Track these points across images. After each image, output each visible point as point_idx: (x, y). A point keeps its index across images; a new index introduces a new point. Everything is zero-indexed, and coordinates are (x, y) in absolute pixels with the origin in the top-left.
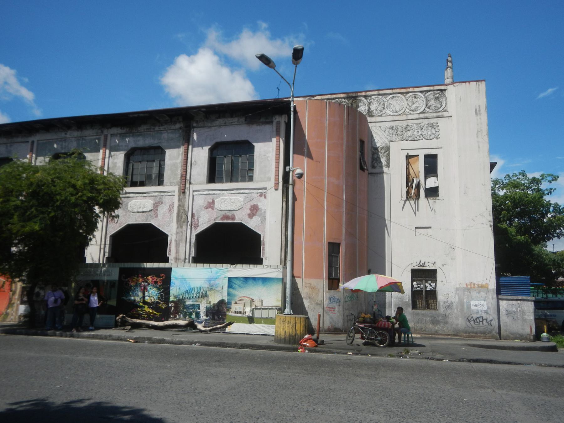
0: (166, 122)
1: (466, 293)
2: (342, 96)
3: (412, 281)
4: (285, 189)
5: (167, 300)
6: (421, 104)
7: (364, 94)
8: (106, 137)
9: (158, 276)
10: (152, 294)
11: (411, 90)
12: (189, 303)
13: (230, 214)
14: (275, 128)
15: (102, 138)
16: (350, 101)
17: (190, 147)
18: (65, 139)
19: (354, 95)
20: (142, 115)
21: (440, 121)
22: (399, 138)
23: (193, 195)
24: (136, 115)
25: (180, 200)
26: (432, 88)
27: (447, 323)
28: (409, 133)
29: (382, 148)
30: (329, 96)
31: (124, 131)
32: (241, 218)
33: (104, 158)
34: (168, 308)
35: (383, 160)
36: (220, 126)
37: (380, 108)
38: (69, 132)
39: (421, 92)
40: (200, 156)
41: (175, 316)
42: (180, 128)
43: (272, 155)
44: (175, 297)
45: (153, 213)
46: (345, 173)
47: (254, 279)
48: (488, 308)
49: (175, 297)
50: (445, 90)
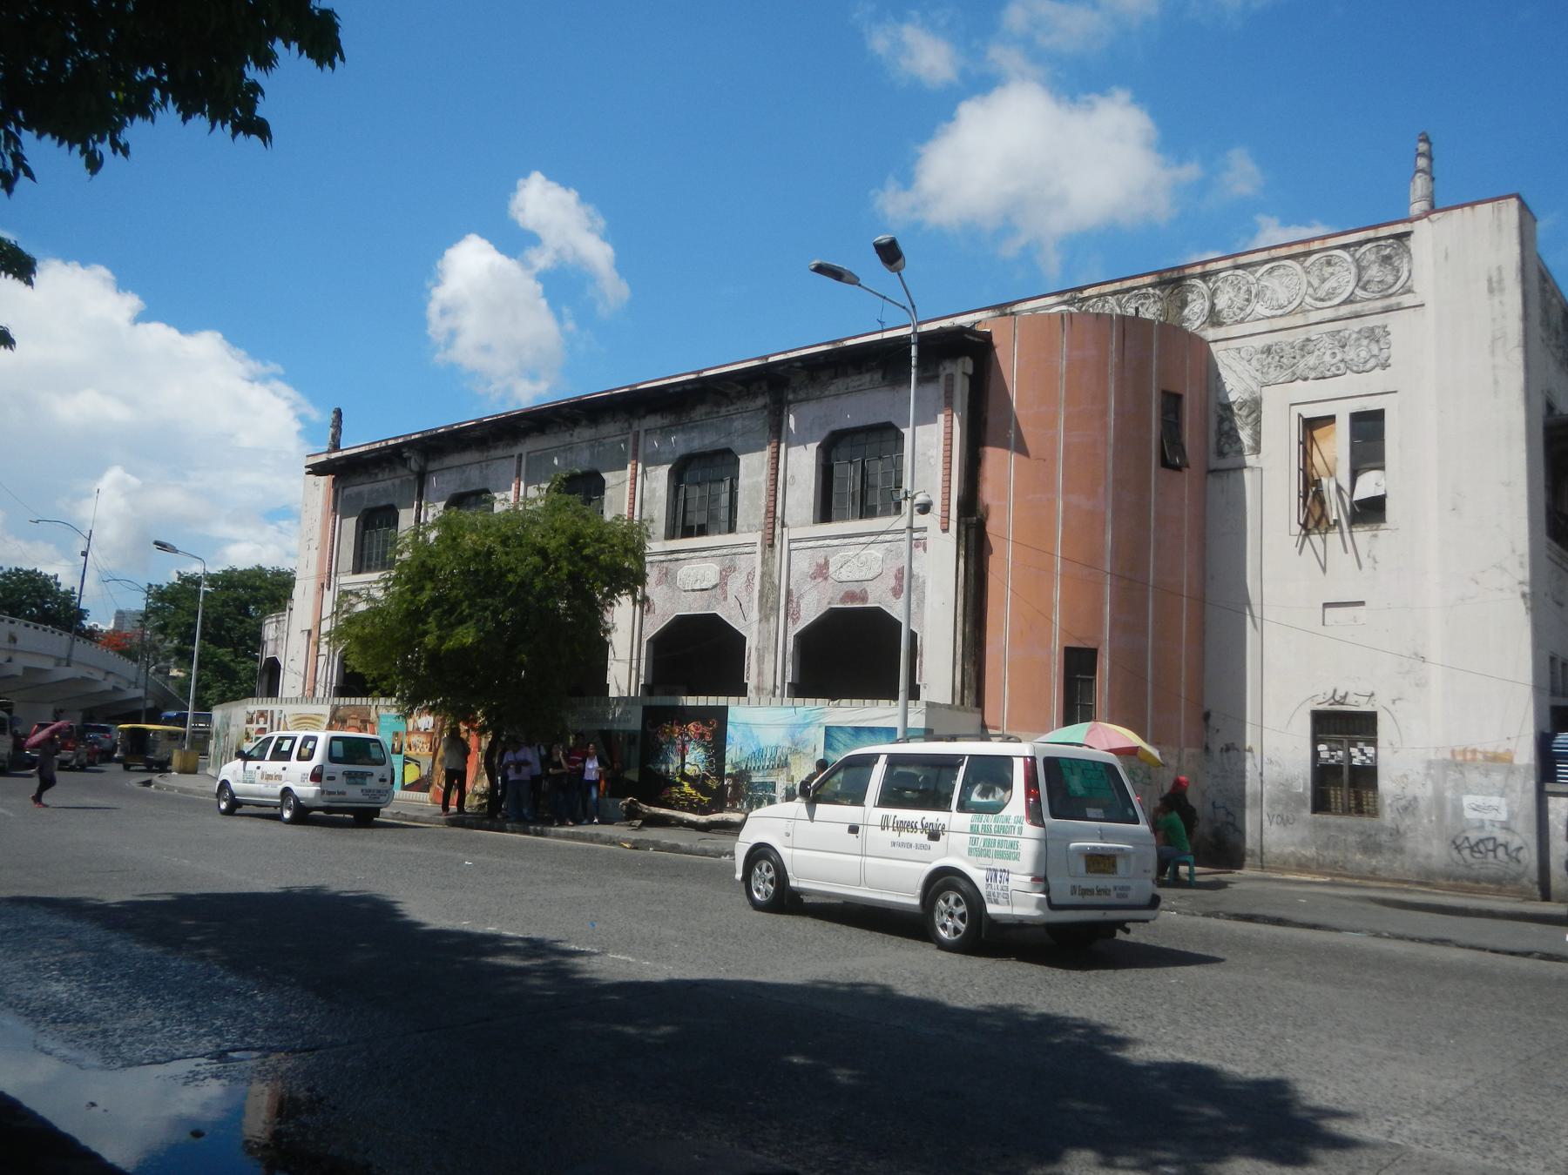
0: (739, 397)
1: (1453, 775)
2: (1148, 280)
3: (1316, 741)
4: (963, 528)
5: (720, 773)
6: (1343, 279)
7: (1198, 269)
8: (637, 435)
9: (705, 723)
10: (695, 760)
11: (1316, 245)
12: (757, 778)
13: (855, 588)
14: (942, 392)
15: (631, 437)
16: (1167, 292)
17: (783, 446)
18: (569, 447)
19: (1175, 275)
20: (689, 387)
21: (1394, 321)
22: (1287, 374)
23: (790, 551)
24: (679, 389)
25: (764, 562)
26: (1371, 234)
27: (1400, 850)
28: (1311, 360)
29: (1243, 405)
30: (1117, 286)
31: (666, 422)
32: (879, 597)
33: (634, 478)
34: (722, 788)
35: (1245, 435)
36: (837, 395)
37: (1239, 302)
38: (577, 431)
39: (1345, 247)
40: (802, 461)
41: (734, 806)
42: (765, 407)
43: (937, 453)
44: (735, 766)
45: (718, 591)
46: (1110, 479)
47: (872, 730)
48: (1512, 815)
49: (735, 766)
50: (1407, 234)
